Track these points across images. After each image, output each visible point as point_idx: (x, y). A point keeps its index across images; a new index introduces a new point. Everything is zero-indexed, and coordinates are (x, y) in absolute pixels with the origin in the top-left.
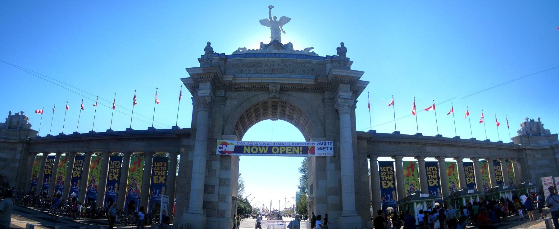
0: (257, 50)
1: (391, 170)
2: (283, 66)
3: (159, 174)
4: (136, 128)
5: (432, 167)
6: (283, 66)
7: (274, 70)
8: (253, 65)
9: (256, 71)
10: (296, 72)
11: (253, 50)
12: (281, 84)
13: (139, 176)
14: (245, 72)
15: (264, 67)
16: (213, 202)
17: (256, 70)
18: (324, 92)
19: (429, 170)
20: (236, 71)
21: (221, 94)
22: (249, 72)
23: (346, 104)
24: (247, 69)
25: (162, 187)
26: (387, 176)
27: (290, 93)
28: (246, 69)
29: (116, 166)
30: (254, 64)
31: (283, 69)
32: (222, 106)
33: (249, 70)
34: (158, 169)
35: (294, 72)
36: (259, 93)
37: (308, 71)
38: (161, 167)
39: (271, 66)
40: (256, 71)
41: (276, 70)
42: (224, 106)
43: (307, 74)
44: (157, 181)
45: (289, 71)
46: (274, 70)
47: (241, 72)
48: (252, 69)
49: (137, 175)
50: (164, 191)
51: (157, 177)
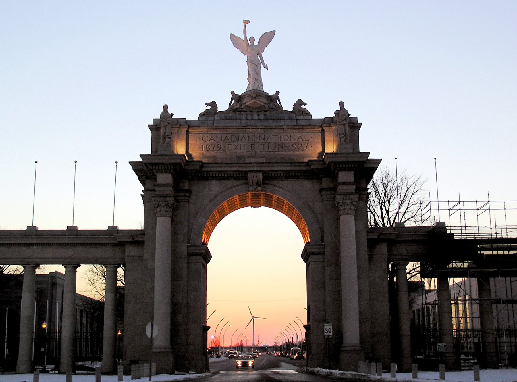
2: (265, 140)
12: (264, 172)
17: (229, 146)
18: (321, 179)
23: (348, 202)
32: (186, 204)
41: (256, 146)
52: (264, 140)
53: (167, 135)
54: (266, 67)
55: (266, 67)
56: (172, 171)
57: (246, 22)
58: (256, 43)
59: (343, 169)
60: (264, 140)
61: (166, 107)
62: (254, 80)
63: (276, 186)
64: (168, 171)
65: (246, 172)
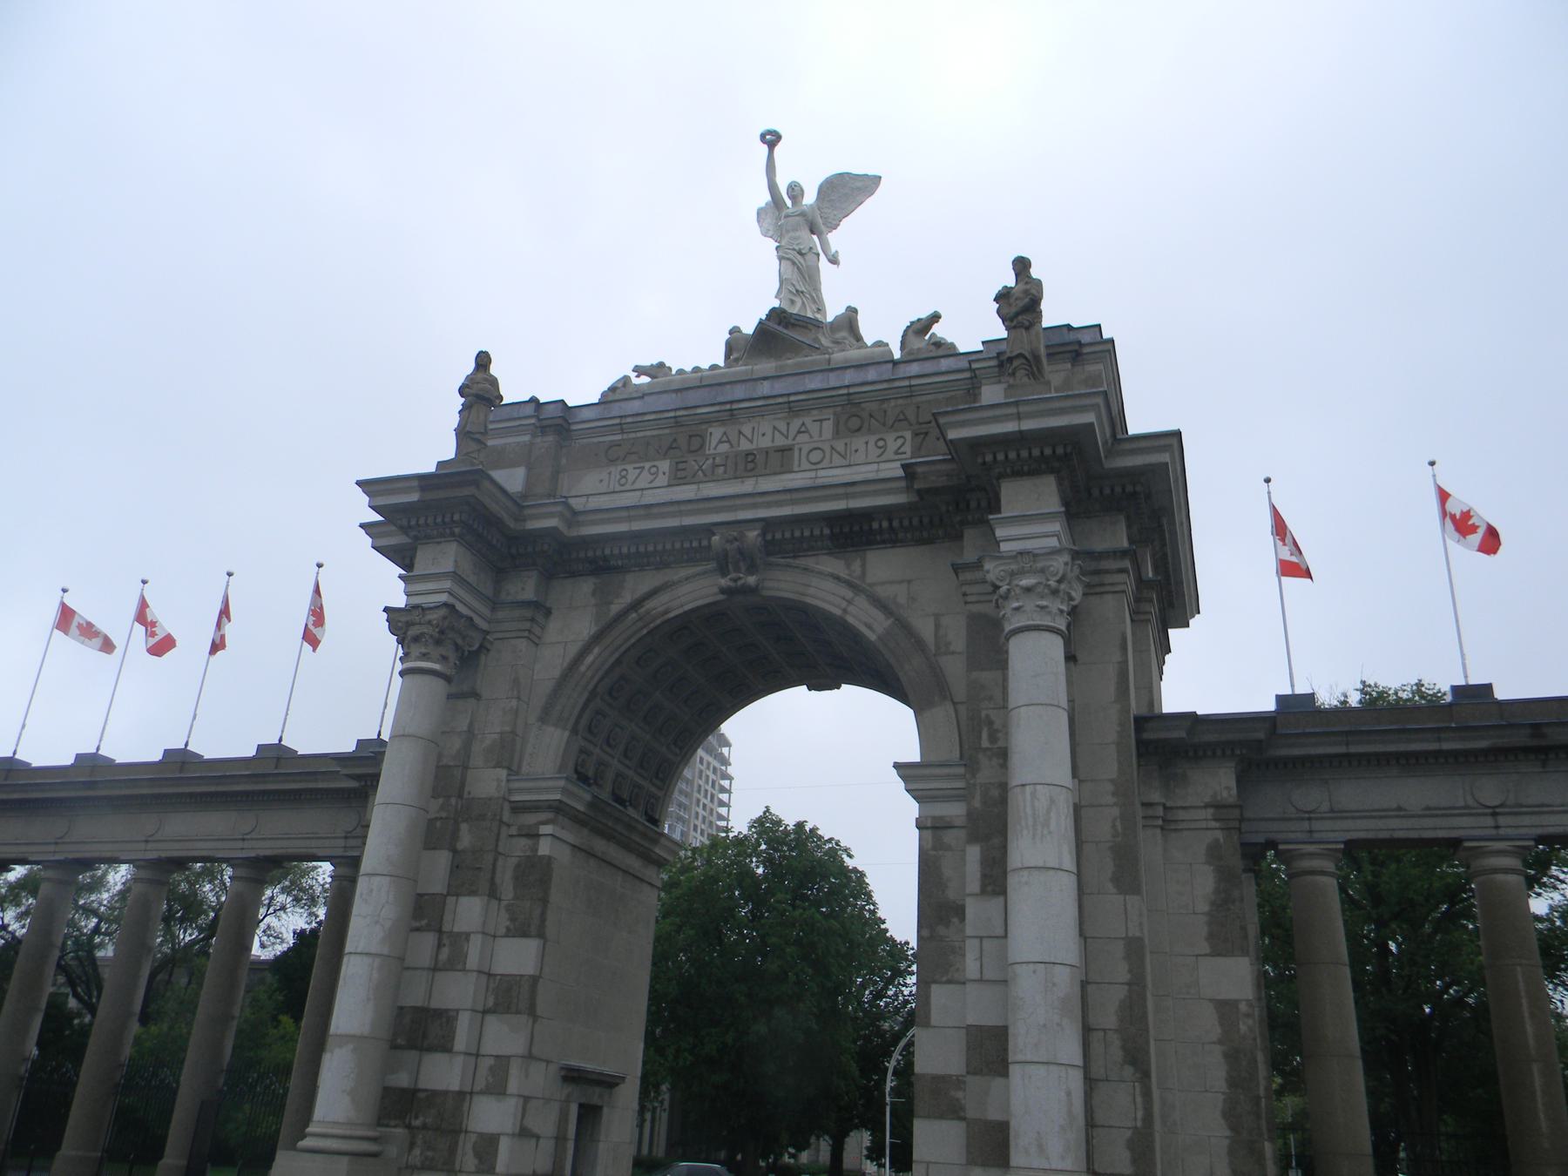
0: (714, 367)
2: (791, 435)
4: (305, 742)
6: (791, 435)
7: (752, 461)
8: (671, 448)
9: (680, 474)
10: (844, 457)
11: (696, 370)
12: (768, 525)
14: (634, 482)
15: (715, 448)
16: (446, 1093)
17: (681, 466)
18: (959, 537)
20: (601, 481)
21: (523, 589)
22: (651, 482)
24: (647, 465)
27: (810, 562)
28: (643, 468)
30: (675, 440)
31: (790, 449)
32: (522, 644)
33: (653, 470)
35: (835, 456)
36: (683, 573)
37: (900, 442)
39: (743, 440)
40: (680, 474)
42: (537, 645)
43: (896, 453)
45: (815, 456)
46: (752, 461)
47: (623, 481)
48: (665, 465)
52: (787, 438)
53: (469, 432)
54: (834, 260)
55: (834, 260)
56: (457, 530)
57: (771, 139)
59: (1020, 472)
60: (787, 438)
61: (483, 360)
62: (790, 292)
63: (812, 571)
64: (448, 531)
65: (709, 529)
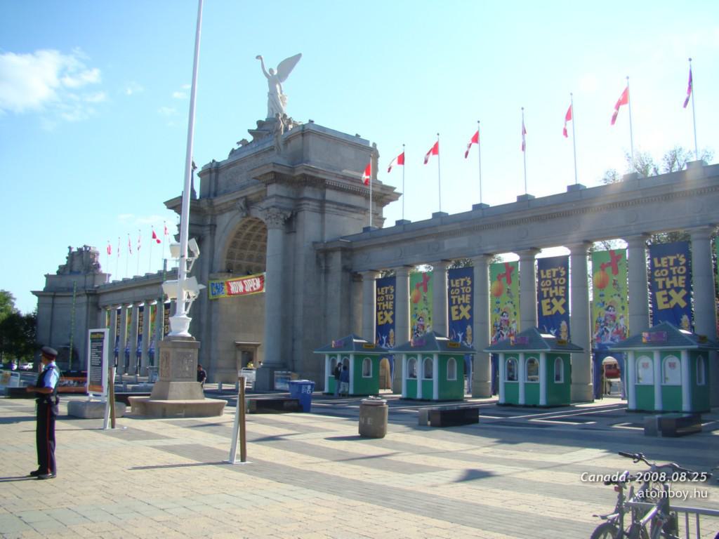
1: (562, 275)
3: (668, 286)
5: (462, 278)
13: (512, 303)
19: (545, 277)
25: (682, 317)
26: (671, 279)
29: (387, 296)
34: (664, 273)
38: (554, 279)
44: (665, 303)
49: (615, 295)
50: (687, 326)
51: (548, 301)
58: (276, 72)
